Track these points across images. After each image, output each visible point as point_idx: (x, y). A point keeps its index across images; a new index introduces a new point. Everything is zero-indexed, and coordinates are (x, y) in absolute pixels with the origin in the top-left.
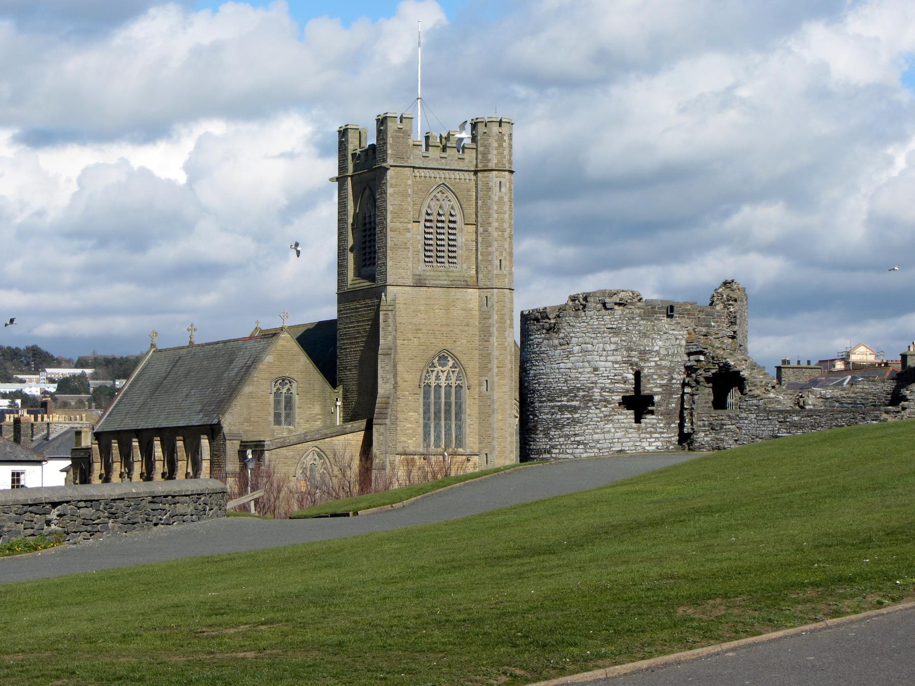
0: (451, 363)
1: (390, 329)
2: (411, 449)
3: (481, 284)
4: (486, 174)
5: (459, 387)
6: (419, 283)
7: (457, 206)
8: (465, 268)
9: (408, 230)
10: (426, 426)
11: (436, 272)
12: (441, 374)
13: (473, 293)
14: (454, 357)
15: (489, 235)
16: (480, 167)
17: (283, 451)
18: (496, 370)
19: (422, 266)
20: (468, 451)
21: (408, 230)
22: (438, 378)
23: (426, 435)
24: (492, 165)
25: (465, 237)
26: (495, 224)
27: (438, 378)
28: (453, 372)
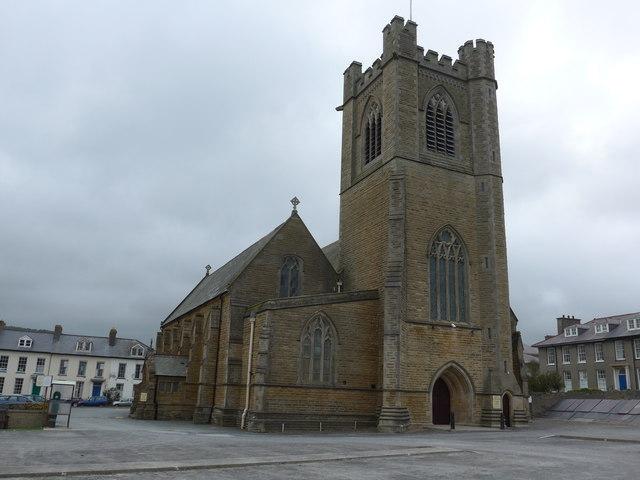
0: (453, 239)
1: (400, 196)
2: (420, 317)
3: (476, 172)
4: (477, 82)
5: (461, 263)
6: (425, 162)
7: (452, 107)
8: (459, 159)
9: (414, 113)
10: (433, 297)
11: (436, 157)
12: (445, 248)
13: (469, 180)
14: (457, 234)
15: (484, 130)
16: (471, 77)
17: (288, 313)
18: (495, 248)
19: (425, 149)
20: (472, 325)
21: (414, 113)
22: (443, 251)
23: (434, 307)
24: (480, 75)
25: (459, 133)
26: (488, 122)
27: (443, 251)
28: (456, 248)
